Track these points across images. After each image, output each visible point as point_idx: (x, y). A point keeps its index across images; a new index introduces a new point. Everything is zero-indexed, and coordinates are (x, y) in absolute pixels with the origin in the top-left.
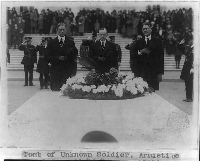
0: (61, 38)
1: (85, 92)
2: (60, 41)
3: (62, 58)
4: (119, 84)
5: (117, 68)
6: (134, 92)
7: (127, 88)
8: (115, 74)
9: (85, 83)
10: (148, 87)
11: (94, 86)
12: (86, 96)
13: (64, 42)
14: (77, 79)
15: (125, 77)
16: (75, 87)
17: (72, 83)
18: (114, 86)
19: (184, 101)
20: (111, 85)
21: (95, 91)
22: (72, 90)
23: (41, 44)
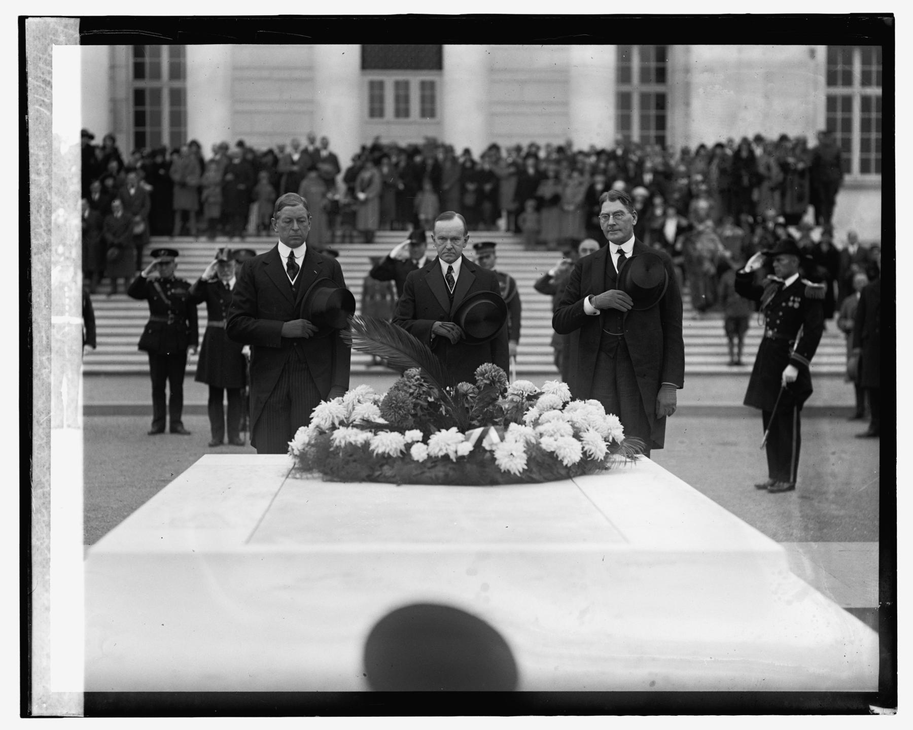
0: (289, 250)
1: (384, 453)
2: (285, 261)
3: (294, 327)
4: (513, 426)
5: (506, 369)
6: (571, 453)
7: (542, 440)
8: (496, 388)
9: (382, 421)
10: (622, 437)
11: (417, 434)
12: (387, 470)
13: (300, 266)
14: (351, 407)
15: (533, 398)
16: (342, 436)
17: (333, 424)
18: (493, 434)
19: (759, 487)
20: (481, 429)
21: (419, 453)
22: (332, 449)
23: (212, 273)
